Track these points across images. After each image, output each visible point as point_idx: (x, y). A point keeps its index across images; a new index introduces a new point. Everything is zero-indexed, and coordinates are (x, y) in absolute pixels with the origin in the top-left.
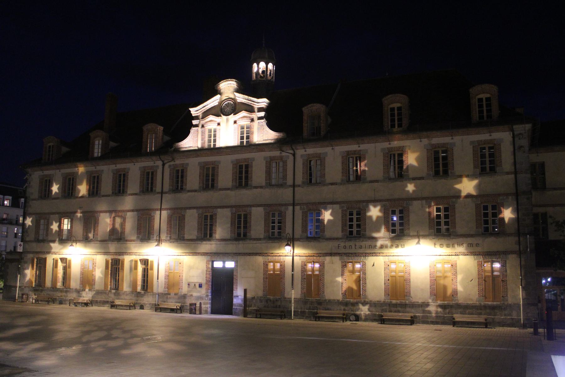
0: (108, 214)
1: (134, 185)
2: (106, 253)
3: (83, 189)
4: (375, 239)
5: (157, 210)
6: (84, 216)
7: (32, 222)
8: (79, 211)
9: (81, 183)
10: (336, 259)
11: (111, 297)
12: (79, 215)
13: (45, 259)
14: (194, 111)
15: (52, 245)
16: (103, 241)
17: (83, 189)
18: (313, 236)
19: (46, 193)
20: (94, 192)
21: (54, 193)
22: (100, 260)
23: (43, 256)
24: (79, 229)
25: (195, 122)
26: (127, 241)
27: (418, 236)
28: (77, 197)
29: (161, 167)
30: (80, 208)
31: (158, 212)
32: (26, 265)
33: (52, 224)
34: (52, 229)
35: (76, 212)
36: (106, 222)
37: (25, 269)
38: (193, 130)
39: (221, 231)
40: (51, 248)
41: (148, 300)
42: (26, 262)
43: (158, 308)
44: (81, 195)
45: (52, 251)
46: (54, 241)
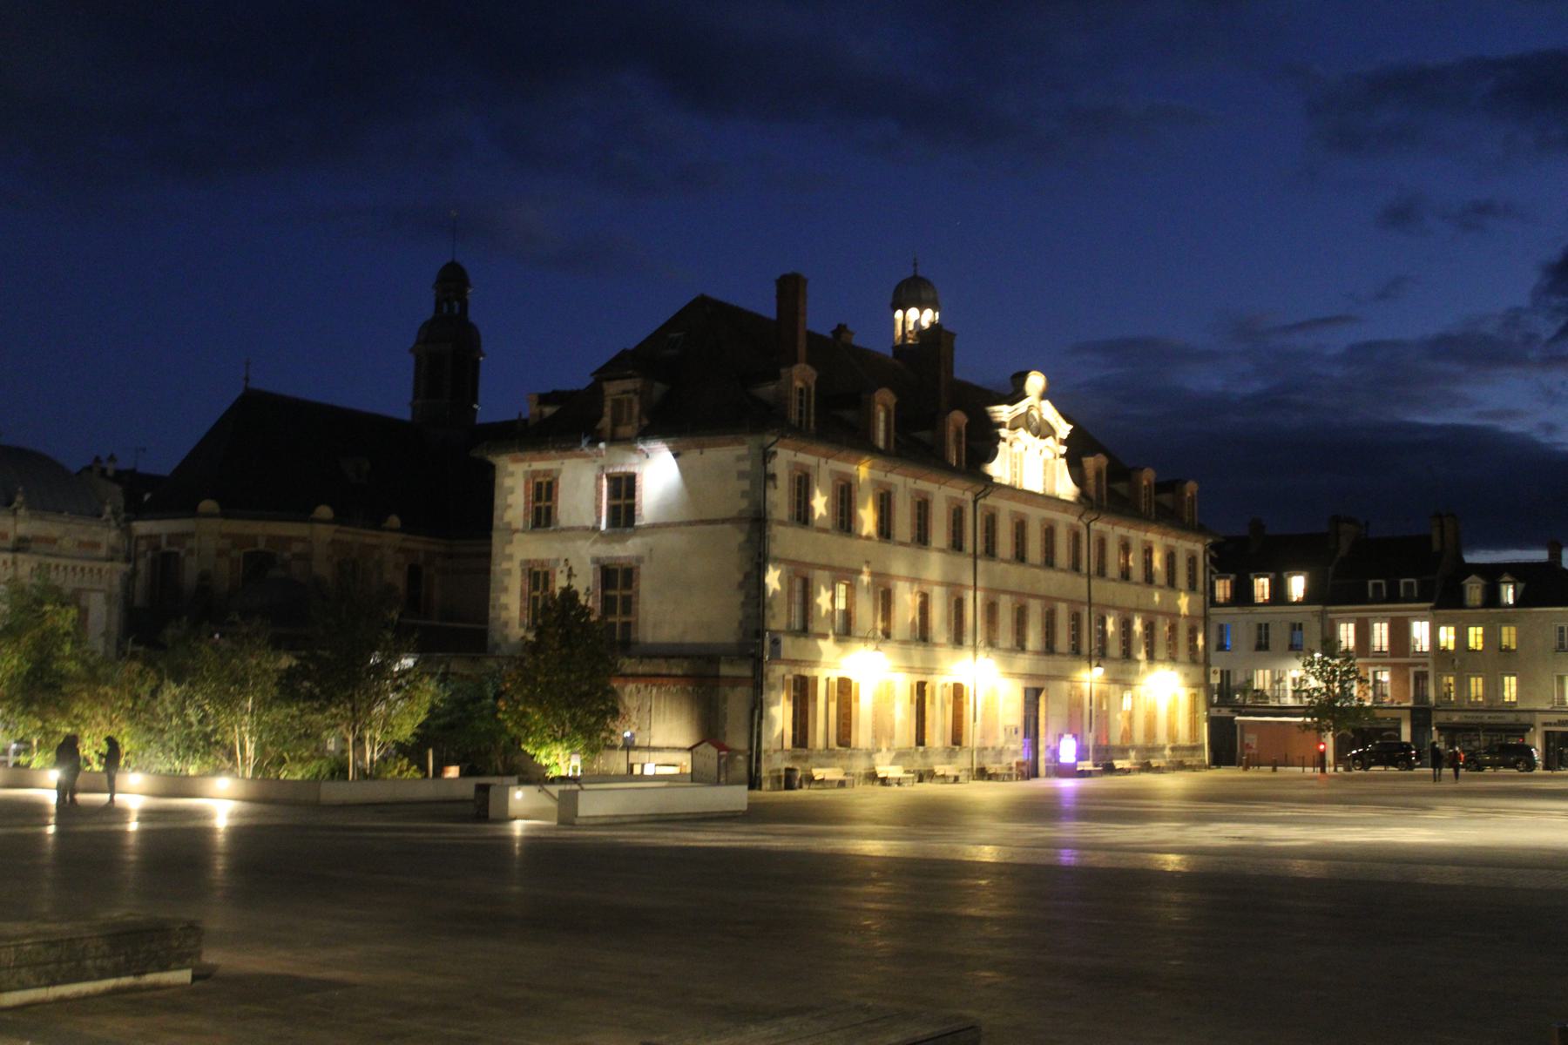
0: (908, 585)
1: (939, 533)
2: (911, 669)
3: (867, 518)
4: (1138, 661)
5: (967, 587)
6: (873, 582)
7: (780, 580)
8: (865, 569)
9: (864, 507)
10: (1117, 687)
11: (919, 764)
12: (865, 578)
13: (815, 680)
14: (1003, 413)
15: (821, 643)
16: (904, 642)
17: (867, 518)
18: (1100, 655)
19: (802, 514)
20: (885, 529)
21: (817, 515)
22: (903, 685)
23: (807, 672)
24: (865, 612)
25: (1003, 432)
26: (935, 645)
27: (1163, 661)
28: (860, 537)
29: (971, 505)
30: (868, 563)
31: (971, 593)
32: (773, 694)
33: (819, 593)
34: (819, 607)
35: (860, 572)
36: (906, 602)
37: (771, 704)
38: (1001, 446)
39: (1034, 639)
40: (819, 653)
41: (963, 762)
42: (772, 687)
43: (982, 774)
44: (864, 533)
45: (824, 659)
46: (825, 636)
